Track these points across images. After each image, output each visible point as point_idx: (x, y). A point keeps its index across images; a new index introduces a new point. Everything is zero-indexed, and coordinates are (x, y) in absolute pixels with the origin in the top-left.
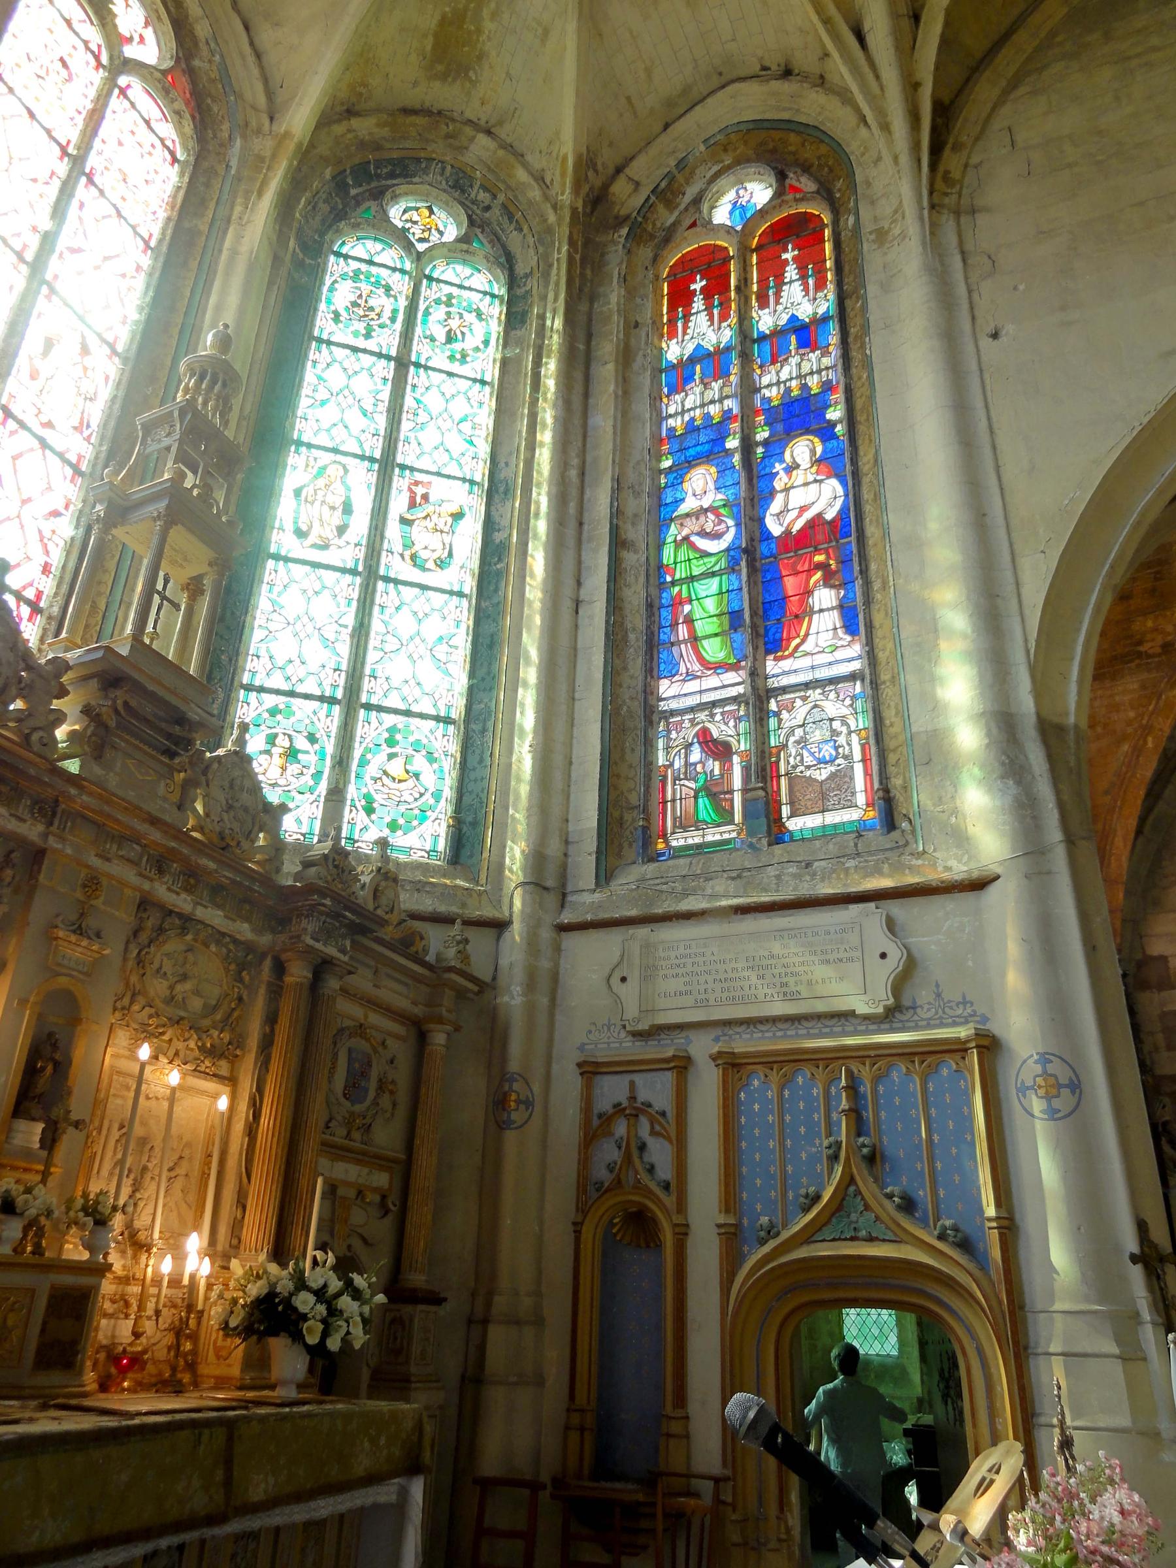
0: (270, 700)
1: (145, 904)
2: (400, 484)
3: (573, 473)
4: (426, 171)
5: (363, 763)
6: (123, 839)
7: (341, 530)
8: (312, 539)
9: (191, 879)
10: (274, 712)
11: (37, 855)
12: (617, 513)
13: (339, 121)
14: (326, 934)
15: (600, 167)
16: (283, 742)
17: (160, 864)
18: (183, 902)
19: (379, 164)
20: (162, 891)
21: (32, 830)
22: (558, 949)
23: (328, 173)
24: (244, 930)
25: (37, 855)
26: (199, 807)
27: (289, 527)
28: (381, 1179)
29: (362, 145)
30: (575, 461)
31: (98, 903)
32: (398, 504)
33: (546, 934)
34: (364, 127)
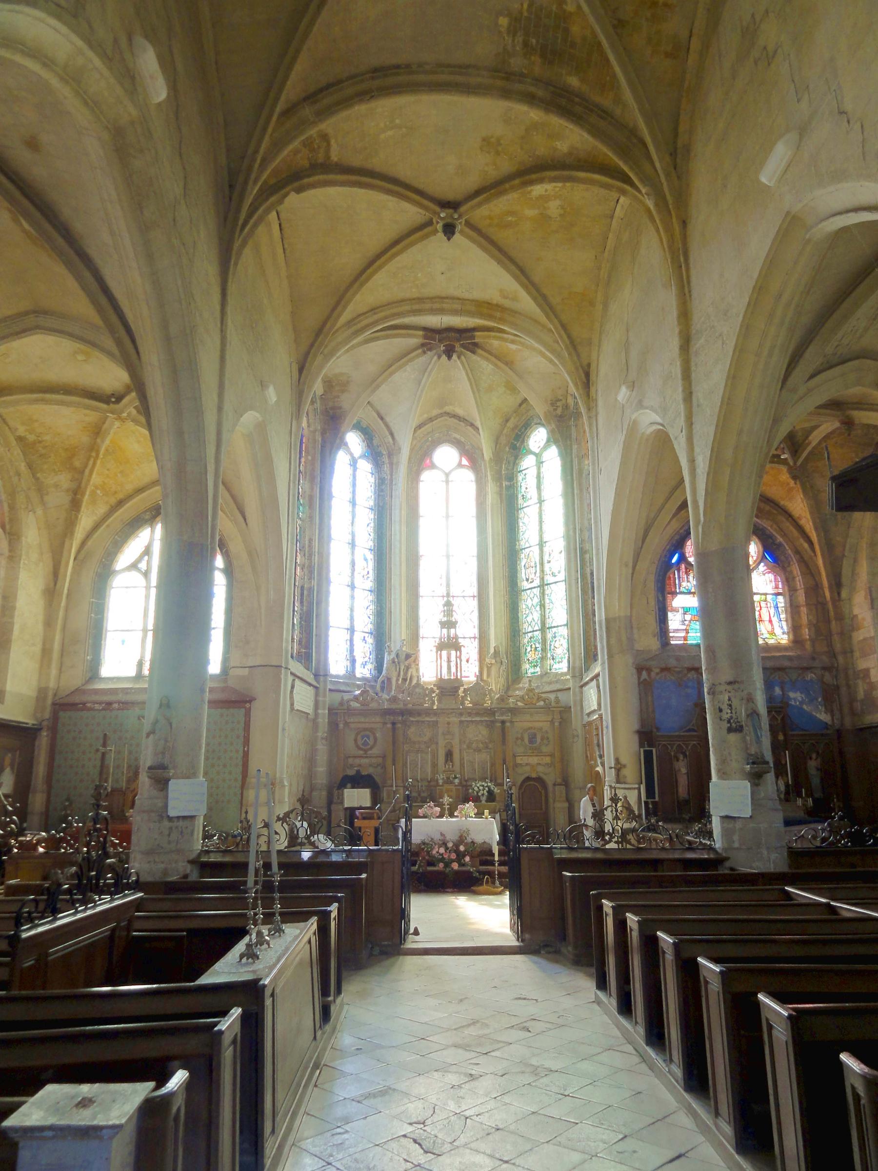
0: (530, 635)
1: (461, 722)
2: (546, 549)
3: (571, 532)
4: (533, 419)
5: (551, 645)
6: (452, 713)
7: (535, 573)
8: (530, 580)
9: (470, 714)
10: (531, 638)
11: (437, 722)
12: (582, 541)
13: (504, 429)
14: (502, 714)
15: (561, 398)
16: (533, 646)
17: (461, 714)
18: (469, 719)
19: (520, 431)
20: (463, 719)
21: (434, 719)
22: (582, 693)
23: (507, 449)
24: (486, 719)
25: (437, 722)
26: (469, 699)
27: (525, 579)
28: (548, 760)
29: (513, 429)
30: (571, 527)
31: (451, 725)
32: (546, 558)
33: (577, 690)
34: (510, 424)
